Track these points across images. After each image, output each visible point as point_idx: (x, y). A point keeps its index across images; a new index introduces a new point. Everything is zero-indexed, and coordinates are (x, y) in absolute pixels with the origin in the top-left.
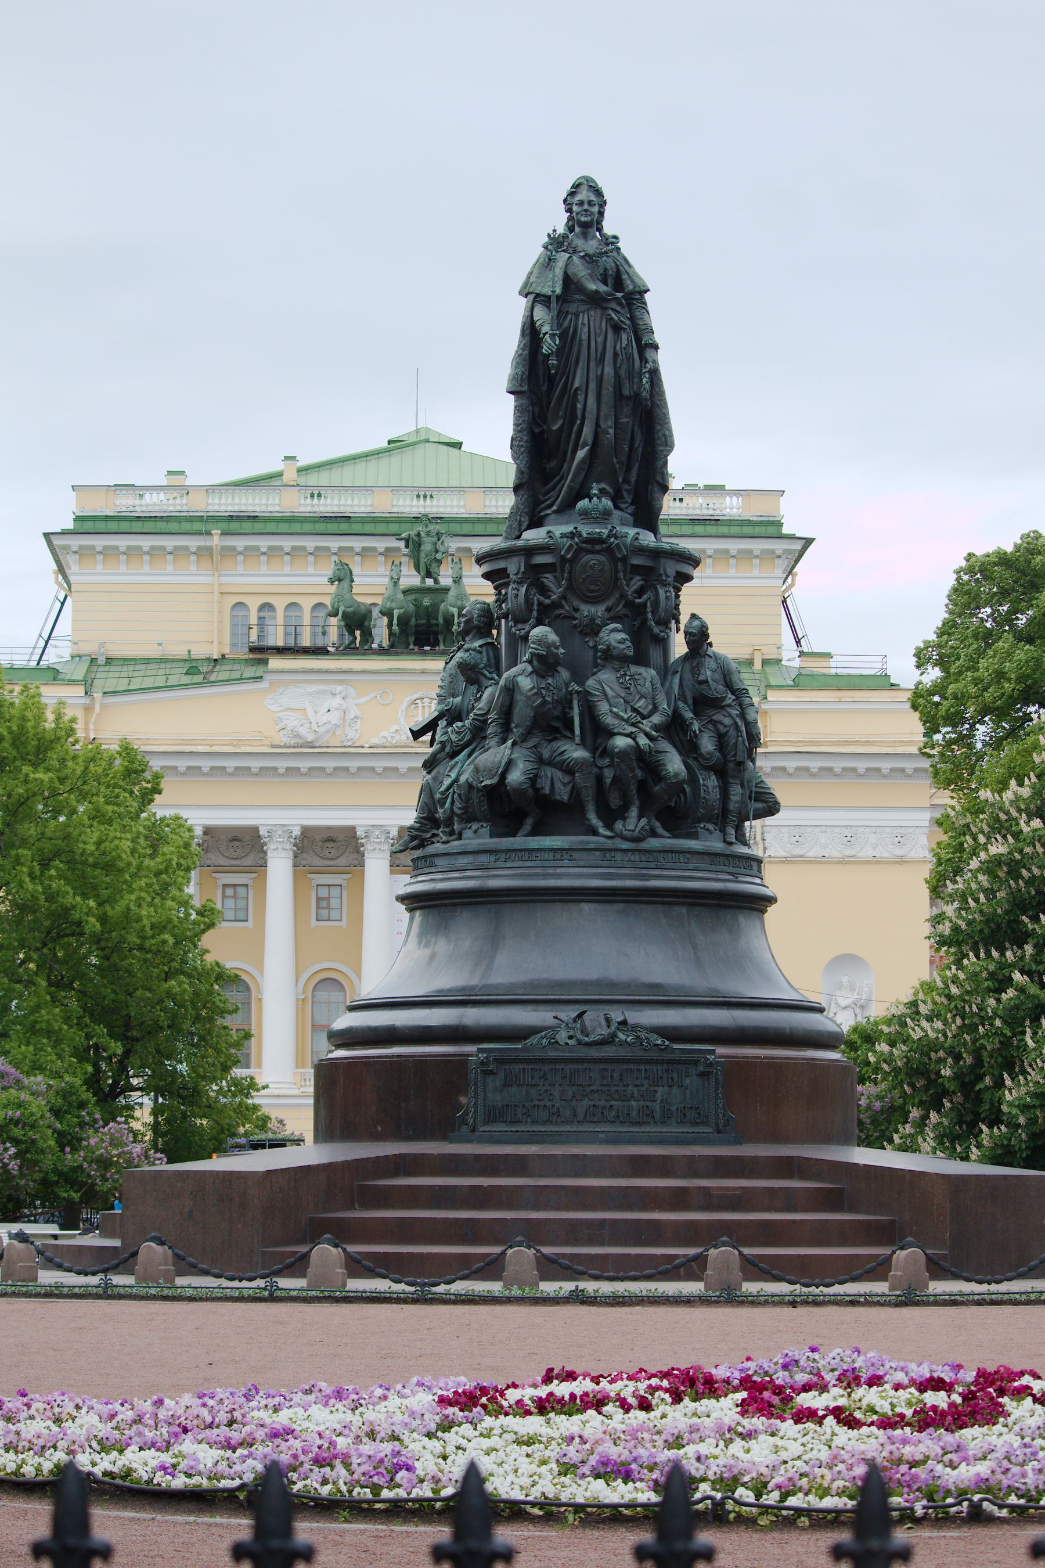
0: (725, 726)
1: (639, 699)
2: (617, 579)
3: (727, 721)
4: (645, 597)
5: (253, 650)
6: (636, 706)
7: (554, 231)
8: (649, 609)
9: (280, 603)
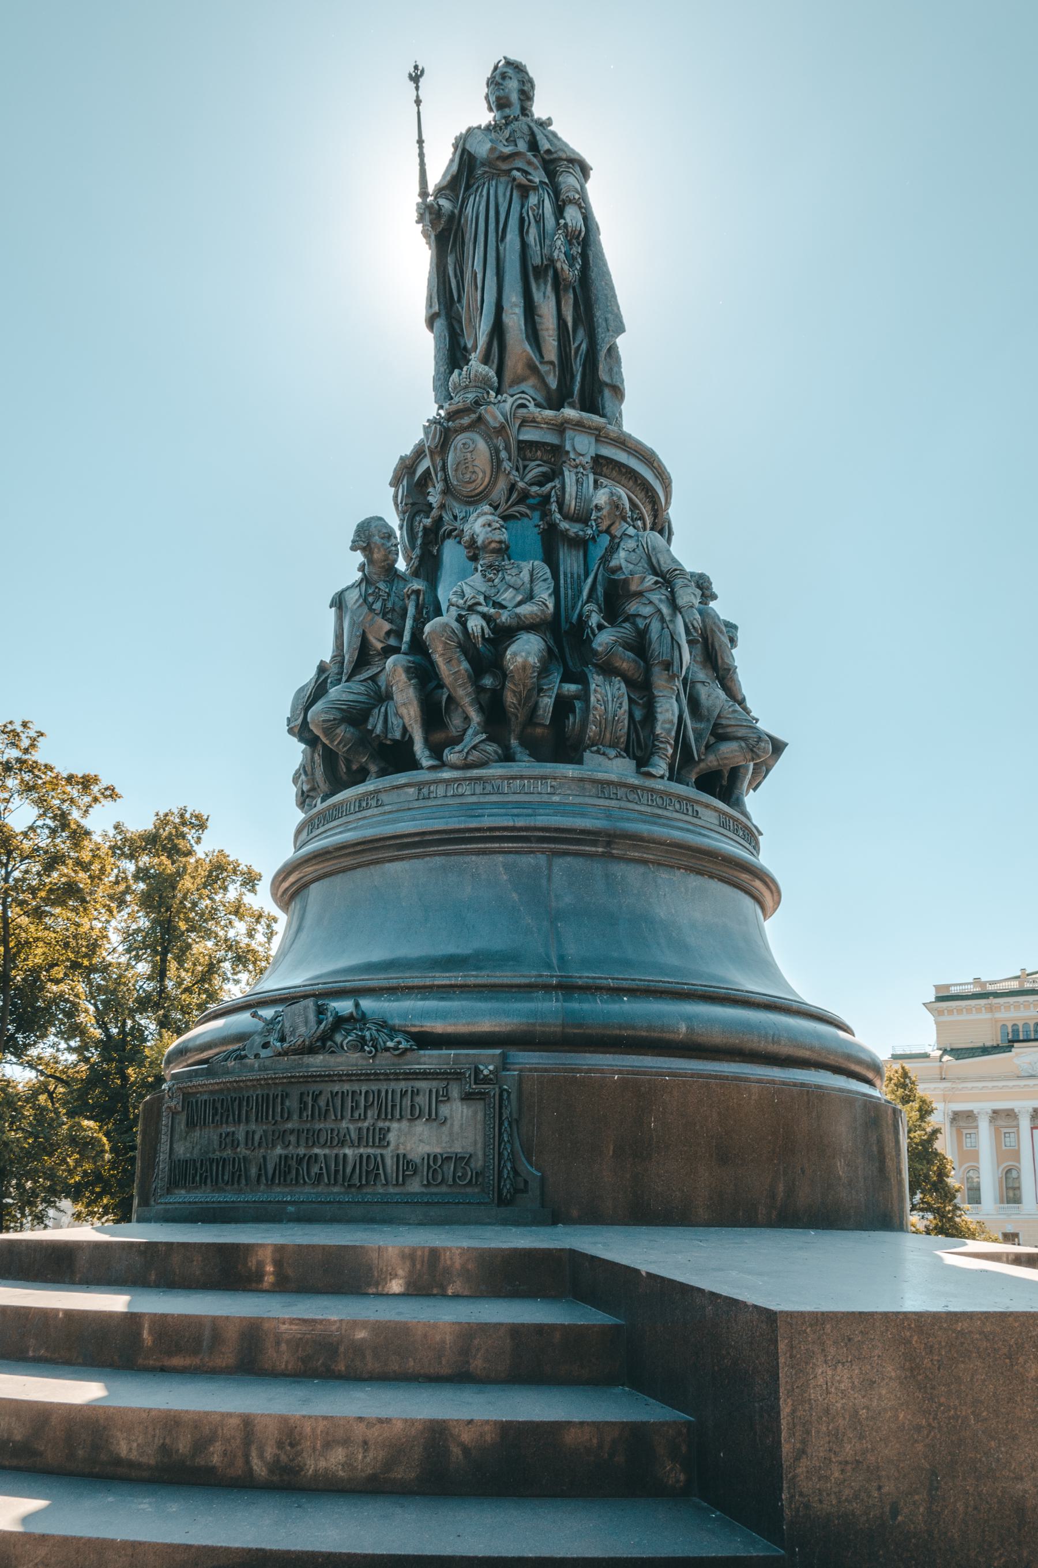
0: (645, 618)
1: (506, 590)
2: (499, 462)
3: (647, 610)
4: (549, 485)
5: (1010, 1041)
6: (499, 600)
7: (416, 67)
8: (552, 500)
9: (1020, 1024)
